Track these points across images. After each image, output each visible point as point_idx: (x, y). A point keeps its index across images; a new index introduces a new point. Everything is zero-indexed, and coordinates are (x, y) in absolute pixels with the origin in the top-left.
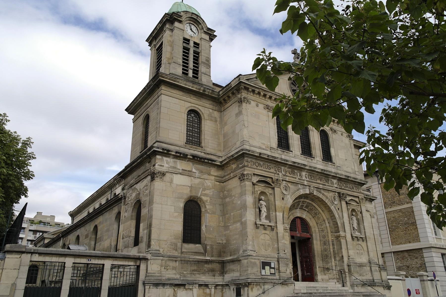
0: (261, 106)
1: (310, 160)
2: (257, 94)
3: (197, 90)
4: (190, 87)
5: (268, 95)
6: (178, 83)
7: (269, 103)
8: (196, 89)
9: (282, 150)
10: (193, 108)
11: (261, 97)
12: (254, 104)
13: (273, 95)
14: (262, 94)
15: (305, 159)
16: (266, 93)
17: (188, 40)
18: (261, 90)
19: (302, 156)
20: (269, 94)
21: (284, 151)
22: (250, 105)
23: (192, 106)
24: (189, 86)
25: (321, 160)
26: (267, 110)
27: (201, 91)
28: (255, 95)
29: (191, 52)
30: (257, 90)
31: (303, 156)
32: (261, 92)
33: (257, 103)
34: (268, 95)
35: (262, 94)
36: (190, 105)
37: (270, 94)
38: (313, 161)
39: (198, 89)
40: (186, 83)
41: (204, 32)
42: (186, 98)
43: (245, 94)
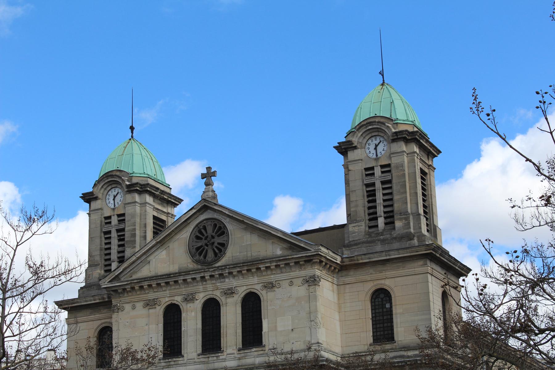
0: (139, 305)
1: (215, 358)
2: (130, 291)
3: (101, 301)
4: (92, 301)
5: (145, 285)
6: (78, 303)
7: (151, 294)
8: (100, 300)
9: (167, 361)
10: (104, 325)
11: (138, 293)
12: (128, 307)
13: (152, 281)
14: (137, 288)
15: (206, 360)
16: (142, 285)
17: (110, 217)
18: (133, 284)
19: (201, 357)
20: (146, 284)
21: (170, 360)
22: (124, 312)
23: (102, 324)
24: (90, 301)
25: (235, 352)
26: (148, 307)
27: (107, 300)
28: (130, 294)
29: (114, 234)
30: (129, 287)
31: (203, 356)
32: (135, 286)
33: (133, 304)
34: (145, 285)
35: (137, 288)
36: (99, 322)
37: (147, 282)
38: (221, 357)
39: (102, 299)
40: (85, 300)
41: (128, 193)
42: (93, 316)
43: (116, 300)
